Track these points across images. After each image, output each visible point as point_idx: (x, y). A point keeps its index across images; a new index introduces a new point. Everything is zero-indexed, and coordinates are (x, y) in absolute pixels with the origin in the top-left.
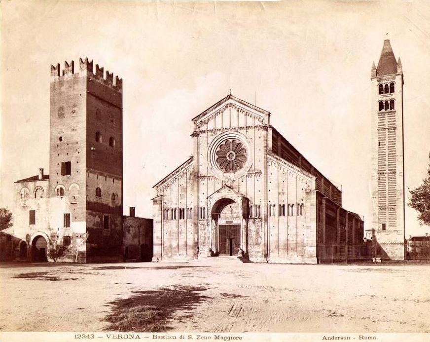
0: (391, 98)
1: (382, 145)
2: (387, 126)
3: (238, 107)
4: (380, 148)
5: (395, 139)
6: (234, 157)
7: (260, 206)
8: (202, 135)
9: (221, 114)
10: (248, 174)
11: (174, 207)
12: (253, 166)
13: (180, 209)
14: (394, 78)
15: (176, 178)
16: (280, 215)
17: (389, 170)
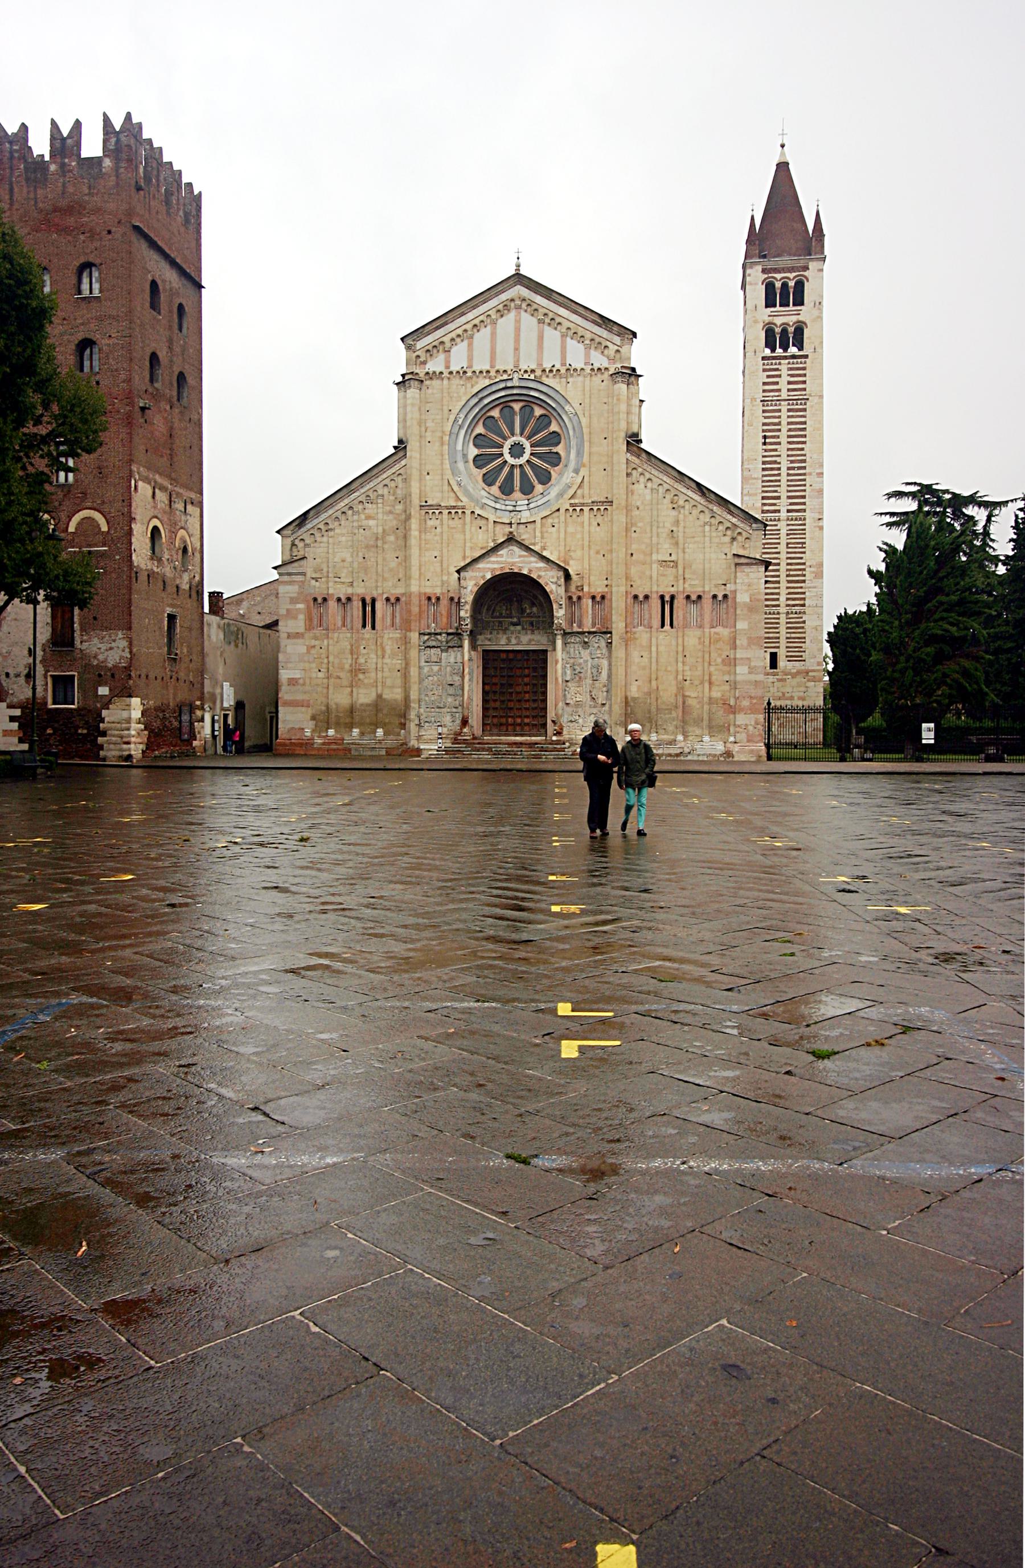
0: (794, 318)
1: (771, 444)
2: (784, 395)
3: (542, 311)
4: (766, 451)
5: (804, 429)
6: (526, 456)
7: (603, 597)
8: (436, 383)
9: (489, 327)
10: (571, 505)
11: (343, 592)
13: (363, 601)
14: (806, 268)
15: (351, 508)
16: (663, 625)
17: (789, 511)
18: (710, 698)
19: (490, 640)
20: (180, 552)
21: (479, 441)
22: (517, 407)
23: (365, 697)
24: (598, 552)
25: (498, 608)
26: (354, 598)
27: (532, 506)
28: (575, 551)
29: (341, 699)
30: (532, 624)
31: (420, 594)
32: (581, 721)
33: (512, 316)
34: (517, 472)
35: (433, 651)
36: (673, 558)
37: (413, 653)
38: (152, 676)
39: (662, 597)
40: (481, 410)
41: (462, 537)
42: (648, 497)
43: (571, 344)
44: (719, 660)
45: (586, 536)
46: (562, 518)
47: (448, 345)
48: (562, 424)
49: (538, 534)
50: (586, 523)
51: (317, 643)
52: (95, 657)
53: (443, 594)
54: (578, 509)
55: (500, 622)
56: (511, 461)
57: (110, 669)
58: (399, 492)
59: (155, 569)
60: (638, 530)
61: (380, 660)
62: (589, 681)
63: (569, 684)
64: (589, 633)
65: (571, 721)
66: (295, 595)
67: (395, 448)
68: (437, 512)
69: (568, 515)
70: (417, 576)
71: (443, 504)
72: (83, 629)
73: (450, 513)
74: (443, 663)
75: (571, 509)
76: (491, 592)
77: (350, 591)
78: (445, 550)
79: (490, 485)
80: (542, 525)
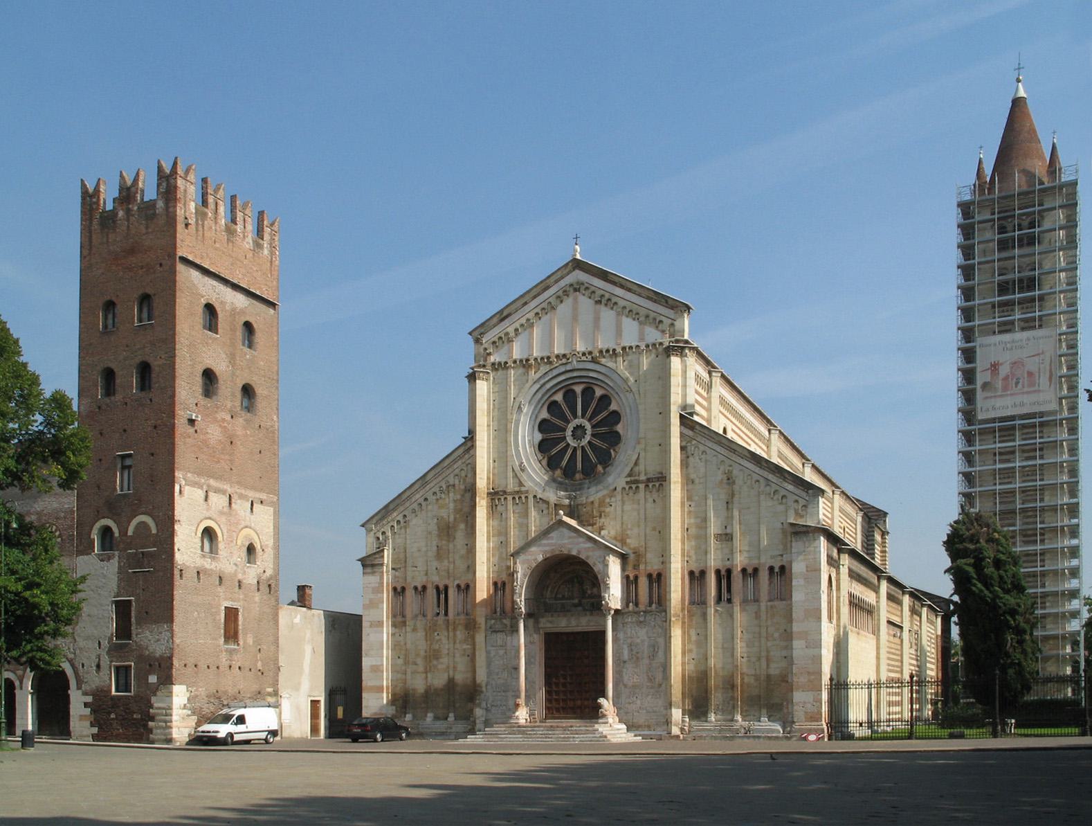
6: (588, 438)
7: (659, 575)
10: (627, 483)
12: (641, 461)
13: (437, 588)
18: (768, 677)
19: (551, 622)
20: (245, 549)
21: (543, 426)
22: (578, 389)
23: (439, 681)
24: (654, 529)
26: (430, 586)
29: (418, 684)
32: (639, 702)
33: (568, 302)
34: (579, 453)
35: (500, 635)
36: (728, 531)
37: (480, 638)
38: (203, 666)
39: (718, 572)
40: (543, 396)
42: (702, 470)
43: (630, 326)
44: (776, 635)
45: (642, 512)
46: (619, 497)
47: (512, 334)
48: (620, 404)
50: (642, 502)
51: (397, 630)
52: (146, 649)
55: (563, 605)
56: (573, 443)
57: (157, 660)
58: (468, 480)
59: (208, 566)
61: (452, 645)
62: (646, 661)
63: (627, 665)
65: (630, 703)
66: (377, 585)
67: (465, 438)
72: (138, 623)
74: (508, 648)
77: (424, 579)
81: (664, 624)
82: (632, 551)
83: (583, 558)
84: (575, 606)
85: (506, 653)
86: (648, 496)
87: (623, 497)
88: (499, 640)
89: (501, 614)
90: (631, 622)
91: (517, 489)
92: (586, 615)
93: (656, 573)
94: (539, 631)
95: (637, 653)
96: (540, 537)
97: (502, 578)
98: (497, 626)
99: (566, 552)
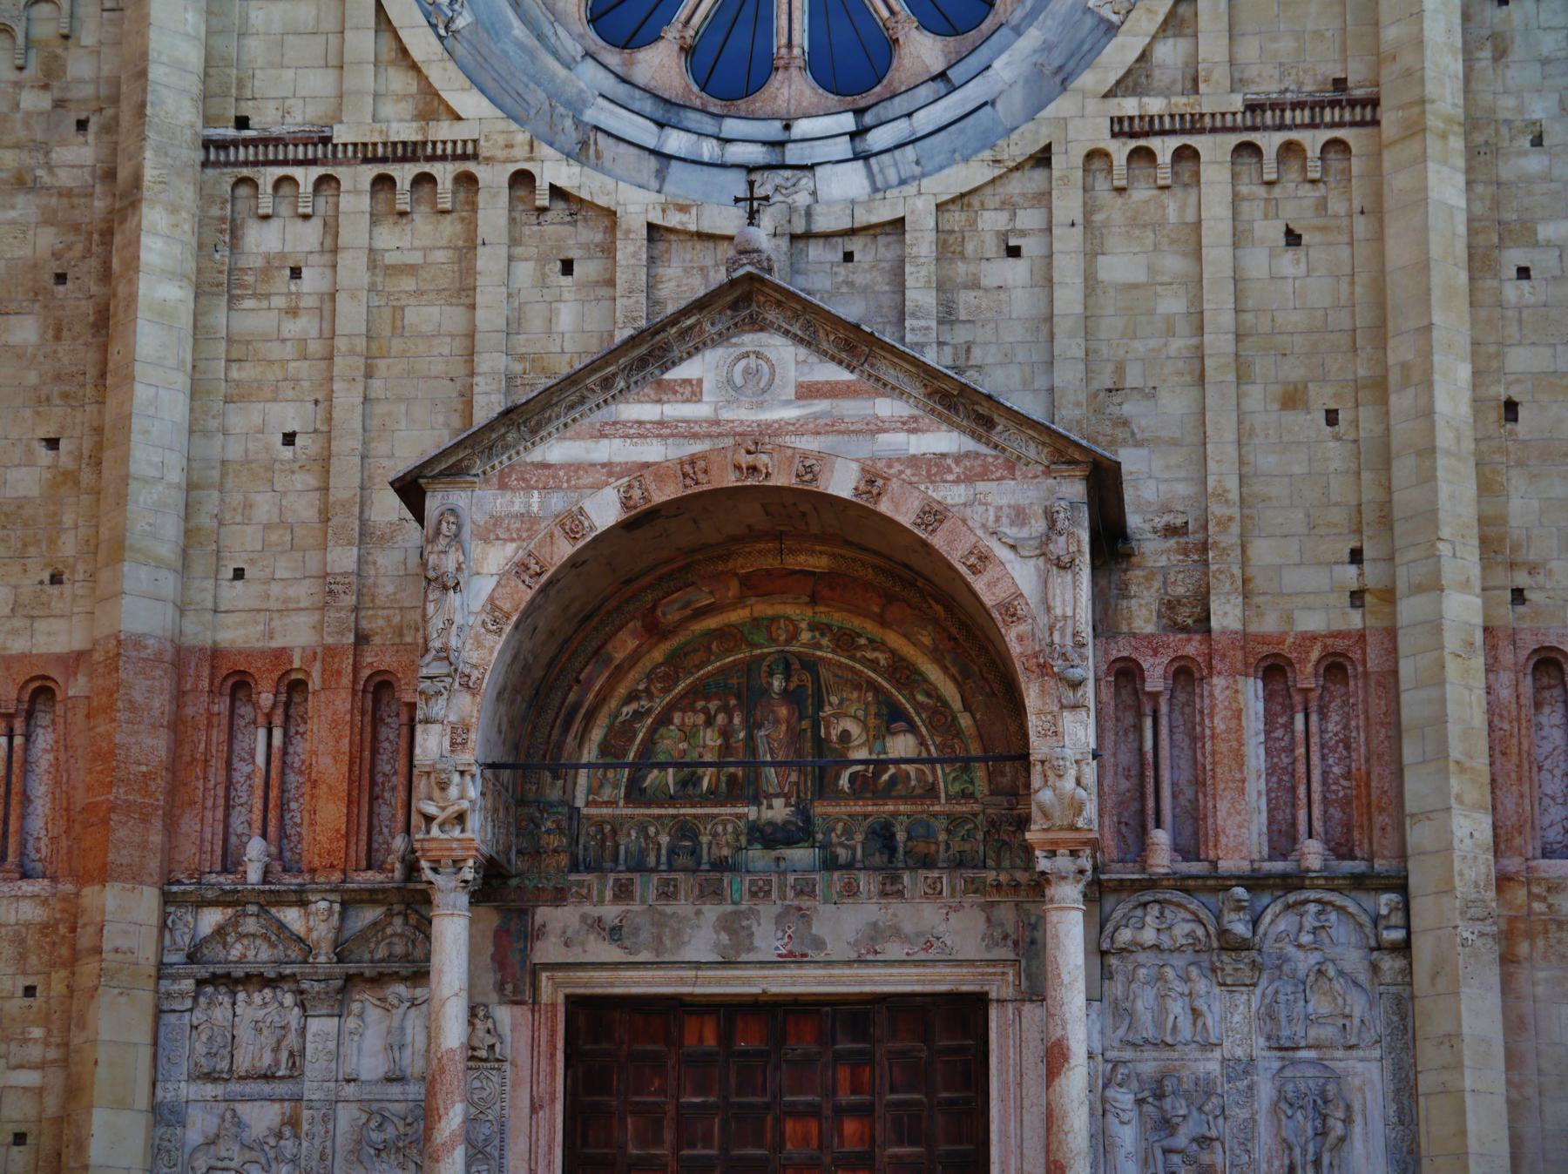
10: (1121, 128)
19: (615, 933)
24: (1292, 399)
25: (670, 743)
27: (878, 139)
28: (1151, 394)
30: (883, 835)
31: (180, 658)
35: (252, 1008)
41: (451, 317)
46: (1068, 204)
49: (920, 296)
53: (330, 651)
54: (1164, 148)
58: (79, 67)
60: (1543, 263)
64: (1255, 882)
68: (306, 177)
69: (1101, 185)
70: (167, 550)
71: (342, 134)
73: (384, 183)
75: (1120, 151)
76: (625, 644)
78: (347, 398)
79: (632, 38)
80: (948, 247)
81: (1390, 964)
82: (1160, 522)
83: (906, 519)
84: (769, 837)
85: (293, 1122)
86: (1249, 210)
87: (1089, 210)
88: (245, 1033)
89: (267, 871)
90: (1156, 947)
91: (406, 132)
92: (851, 891)
93: (1315, 655)
94: (535, 988)
95: (1204, 1141)
96: (607, 383)
97: (281, 654)
98: (235, 953)
99: (782, 479)
